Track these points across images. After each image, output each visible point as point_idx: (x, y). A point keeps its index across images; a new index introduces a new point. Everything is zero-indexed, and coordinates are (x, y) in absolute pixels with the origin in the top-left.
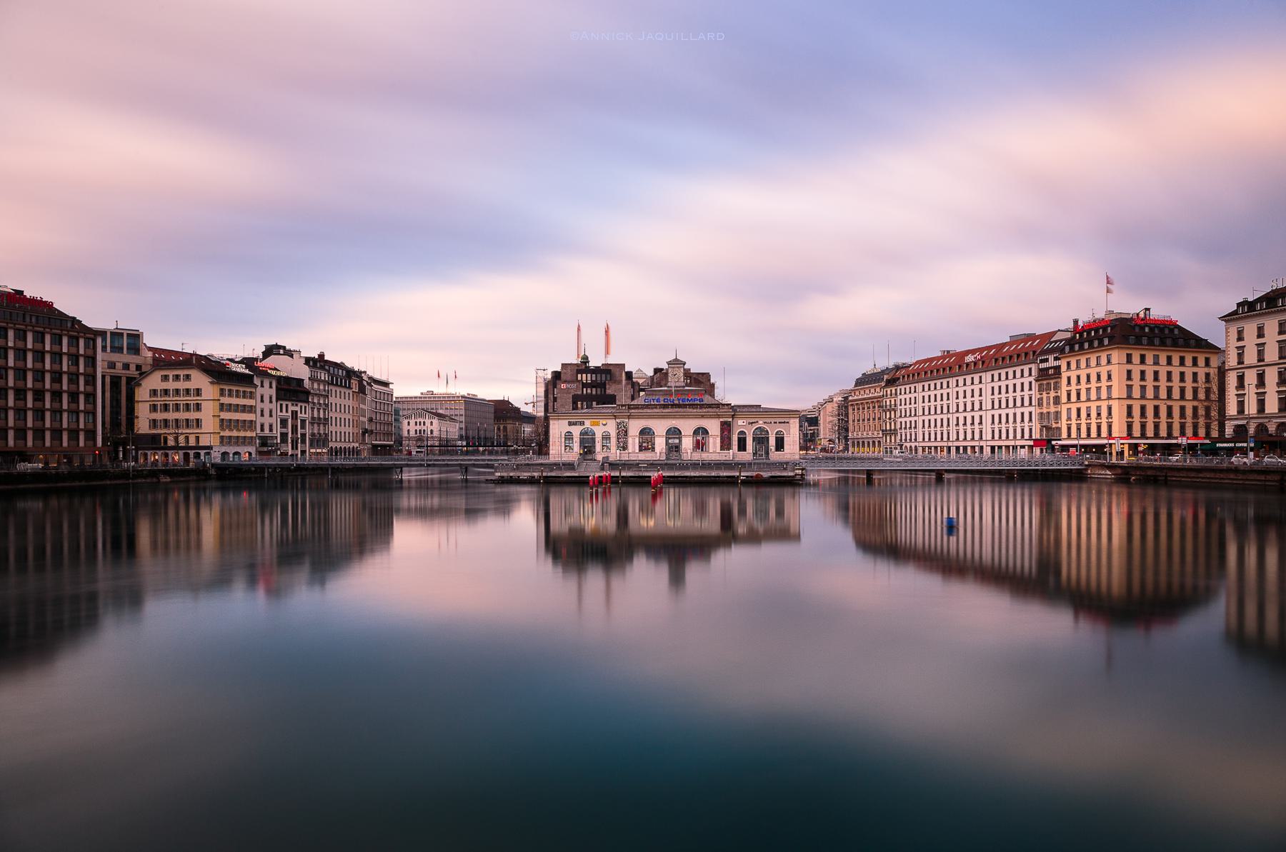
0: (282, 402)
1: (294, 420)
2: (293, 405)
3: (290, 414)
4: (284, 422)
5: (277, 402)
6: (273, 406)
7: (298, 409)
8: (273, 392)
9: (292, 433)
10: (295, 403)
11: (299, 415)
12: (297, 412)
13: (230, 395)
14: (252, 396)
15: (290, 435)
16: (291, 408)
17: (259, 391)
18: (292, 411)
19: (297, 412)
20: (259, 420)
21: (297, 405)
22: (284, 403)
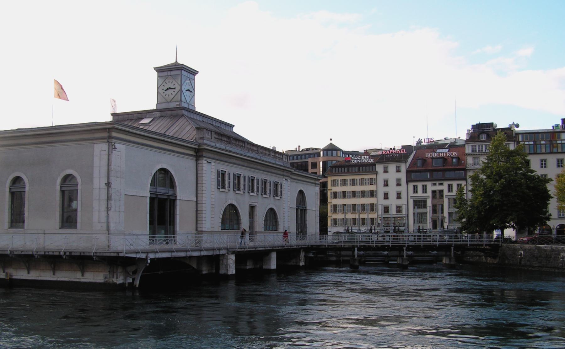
0: (415, 184)
1: (436, 201)
2: (435, 184)
3: (429, 193)
4: (420, 204)
5: (408, 185)
6: (403, 189)
7: (445, 187)
8: (403, 176)
9: (434, 211)
10: (437, 183)
11: (446, 193)
12: (441, 192)
13: (362, 184)
14: (372, 181)
15: (429, 215)
16: (430, 187)
17: (381, 177)
18: (434, 192)
19: (441, 192)
20: (382, 202)
21: (441, 184)
22: (420, 185)
